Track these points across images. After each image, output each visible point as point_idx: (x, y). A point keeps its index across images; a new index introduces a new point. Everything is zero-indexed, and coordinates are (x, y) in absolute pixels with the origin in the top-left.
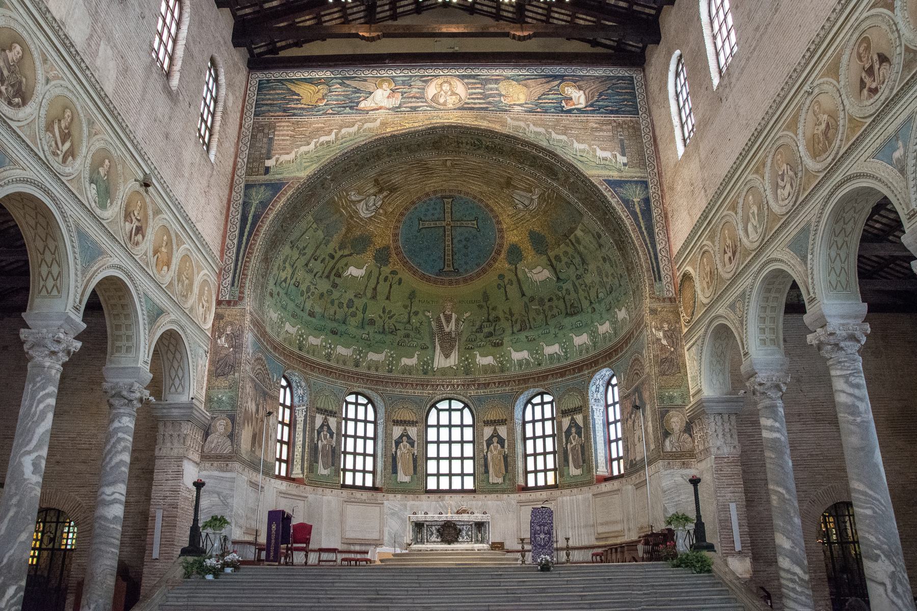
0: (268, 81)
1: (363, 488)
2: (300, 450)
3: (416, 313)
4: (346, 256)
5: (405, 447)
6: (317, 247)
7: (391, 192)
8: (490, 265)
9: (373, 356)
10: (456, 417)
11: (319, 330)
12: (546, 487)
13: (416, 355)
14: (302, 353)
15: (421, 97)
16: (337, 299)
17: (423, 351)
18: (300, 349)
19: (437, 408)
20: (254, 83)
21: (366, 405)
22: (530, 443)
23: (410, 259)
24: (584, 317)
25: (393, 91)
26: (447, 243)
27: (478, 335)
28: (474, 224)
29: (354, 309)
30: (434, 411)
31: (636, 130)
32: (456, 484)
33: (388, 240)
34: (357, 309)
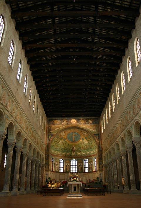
0: (50, 119)
1: (62, 172)
9: (63, 153)
10: (75, 162)
11: (56, 150)
12: (87, 172)
14: (54, 154)
15: (70, 122)
20: (48, 119)
22: (85, 166)
24: (92, 149)
25: (67, 121)
30: (71, 161)
31: (98, 126)
32: (75, 172)
33: (65, 138)
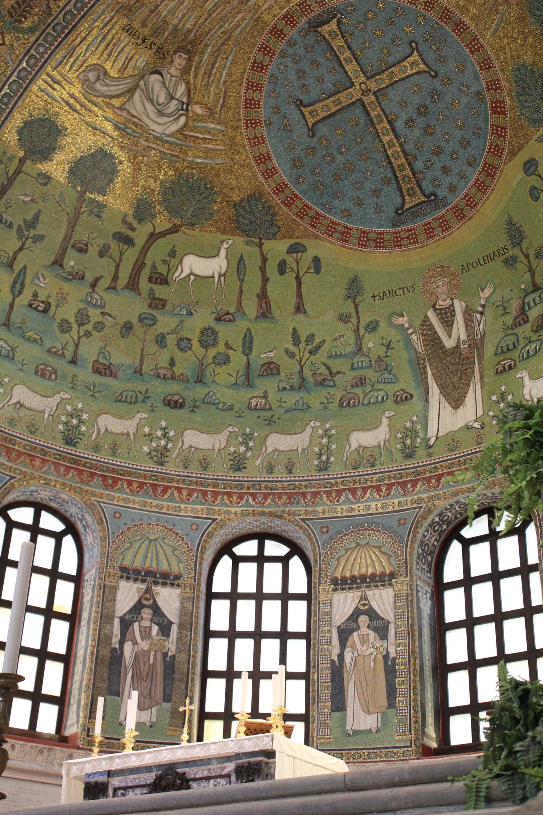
2: (80, 669)
3: (373, 327)
4: (164, 234)
5: (364, 640)
6: (73, 222)
7: (190, 54)
8: (497, 151)
13: (385, 421)
14: (80, 451)
16: (173, 332)
17: (402, 407)
18: (69, 442)
19: (462, 539)
21: (284, 560)
23: (323, 206)
26: (385, 139)
27: (526, 330)
28: (414, 64)
29: (221, 348)
34: (227, 344)
